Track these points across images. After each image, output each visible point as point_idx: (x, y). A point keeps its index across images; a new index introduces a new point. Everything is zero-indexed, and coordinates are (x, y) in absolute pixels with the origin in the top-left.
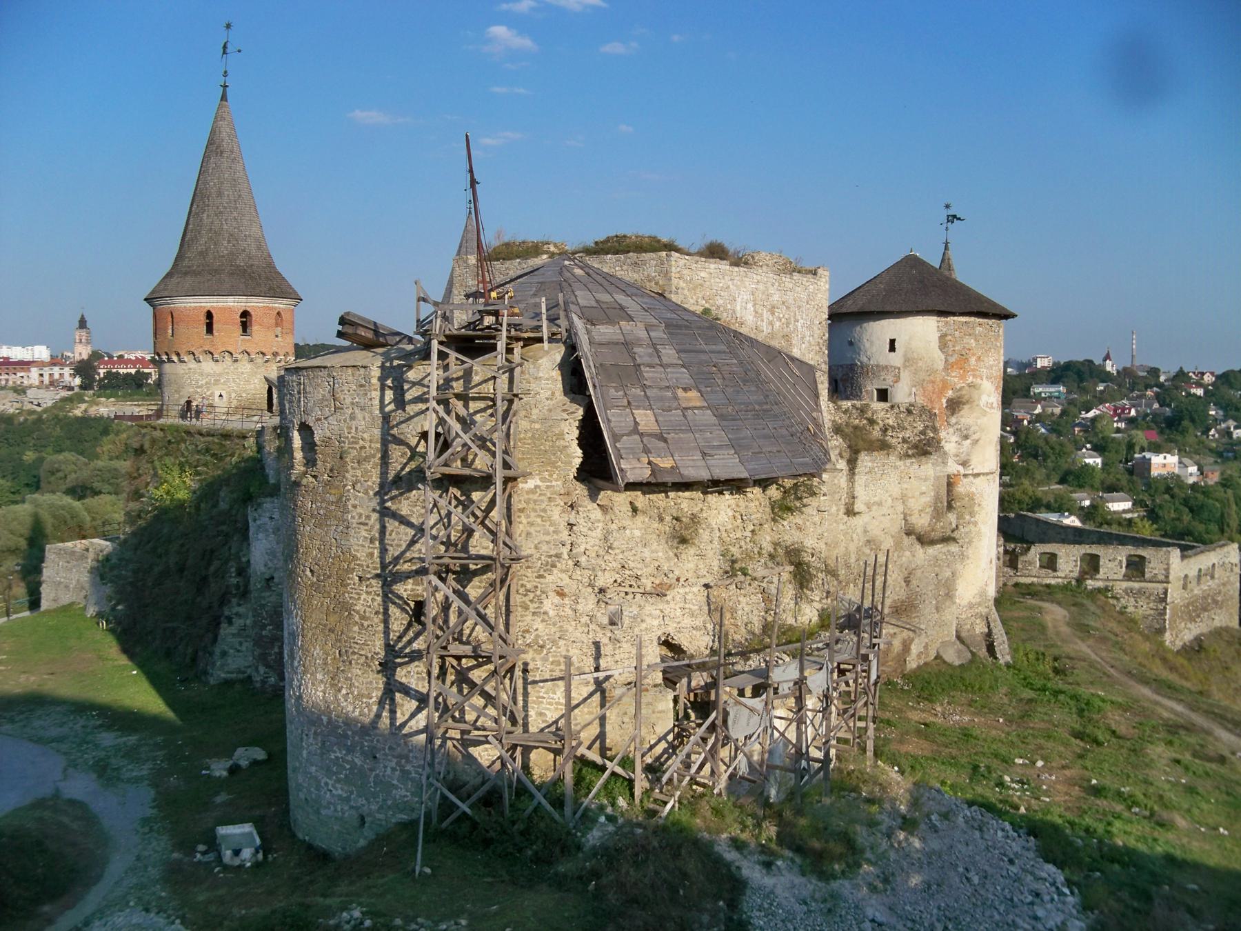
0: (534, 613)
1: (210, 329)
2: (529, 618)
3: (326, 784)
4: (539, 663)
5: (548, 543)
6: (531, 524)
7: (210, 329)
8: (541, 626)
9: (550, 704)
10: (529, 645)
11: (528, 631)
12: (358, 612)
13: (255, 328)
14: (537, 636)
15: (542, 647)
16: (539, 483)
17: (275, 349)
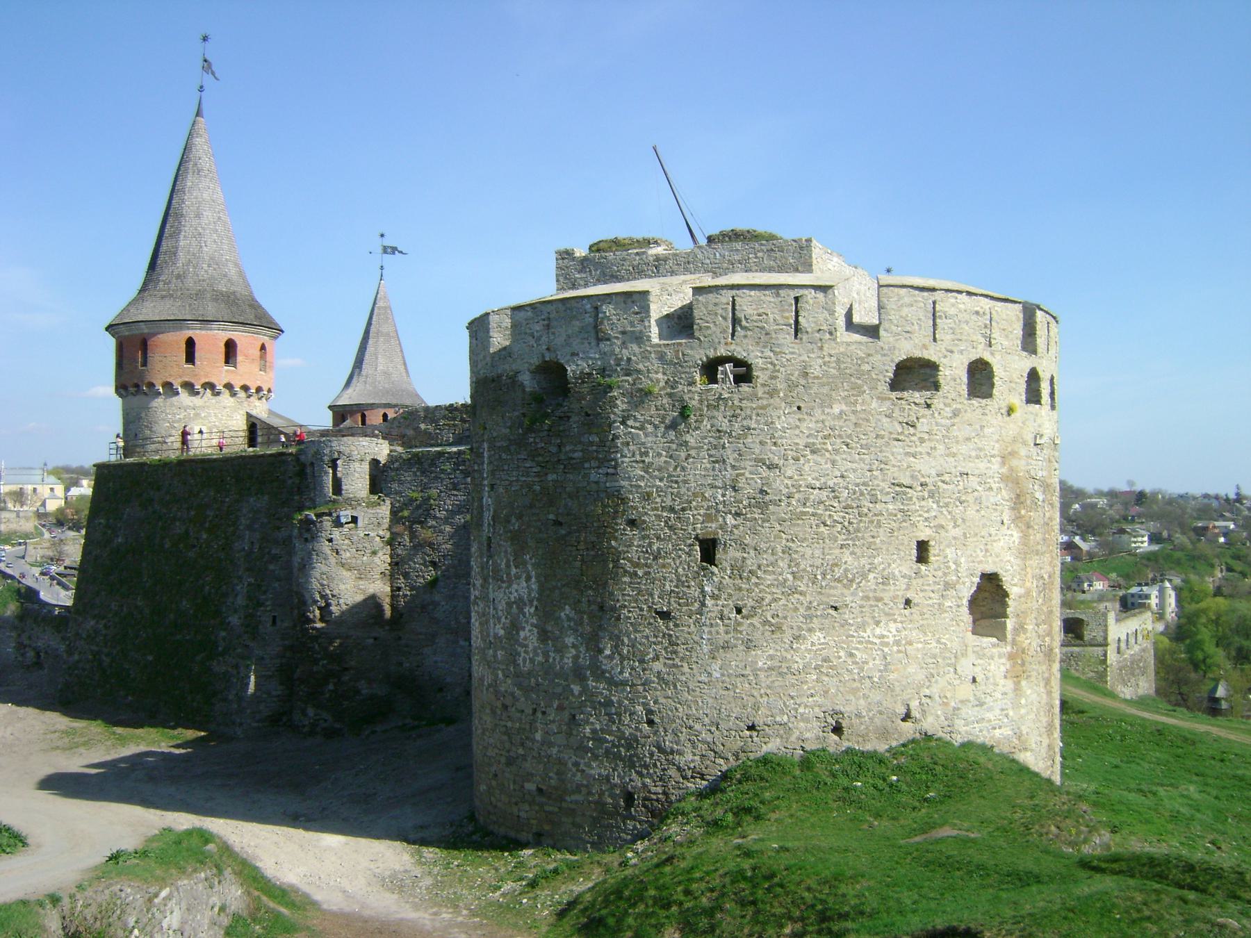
0: (842, 547)
1: (190, 358)
2: (837, 551)
3: (576, 764)
4: (848, 599)
5: (855, 471)
6: (836, 451)
7: (190, 358)
8: (850, 559)
9: (859, 642)
10: (838, 580)
11: (836, 565)
12: (630, 560)
13: (240, 358)
14: (846, 570)
15: (852, 581)
16: (844, 407)
17: (259, 383)
